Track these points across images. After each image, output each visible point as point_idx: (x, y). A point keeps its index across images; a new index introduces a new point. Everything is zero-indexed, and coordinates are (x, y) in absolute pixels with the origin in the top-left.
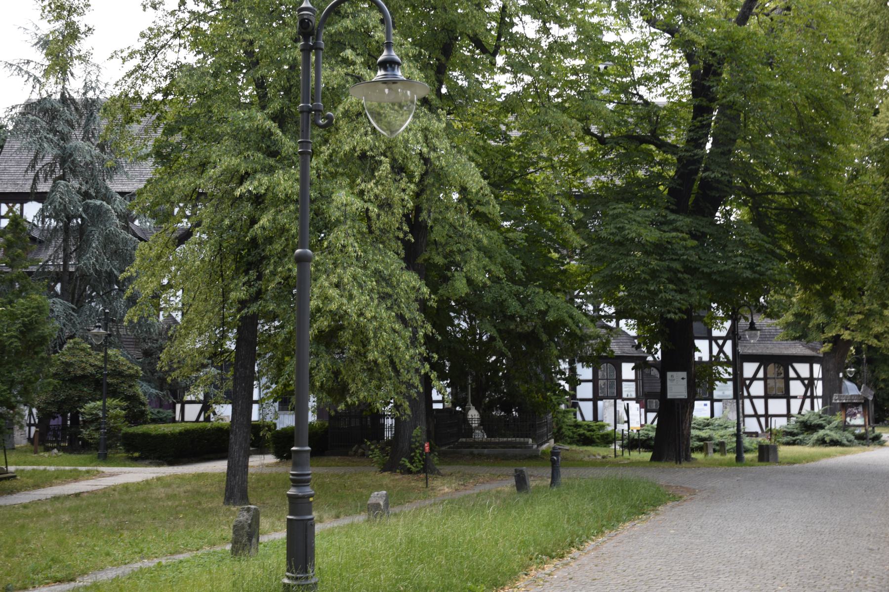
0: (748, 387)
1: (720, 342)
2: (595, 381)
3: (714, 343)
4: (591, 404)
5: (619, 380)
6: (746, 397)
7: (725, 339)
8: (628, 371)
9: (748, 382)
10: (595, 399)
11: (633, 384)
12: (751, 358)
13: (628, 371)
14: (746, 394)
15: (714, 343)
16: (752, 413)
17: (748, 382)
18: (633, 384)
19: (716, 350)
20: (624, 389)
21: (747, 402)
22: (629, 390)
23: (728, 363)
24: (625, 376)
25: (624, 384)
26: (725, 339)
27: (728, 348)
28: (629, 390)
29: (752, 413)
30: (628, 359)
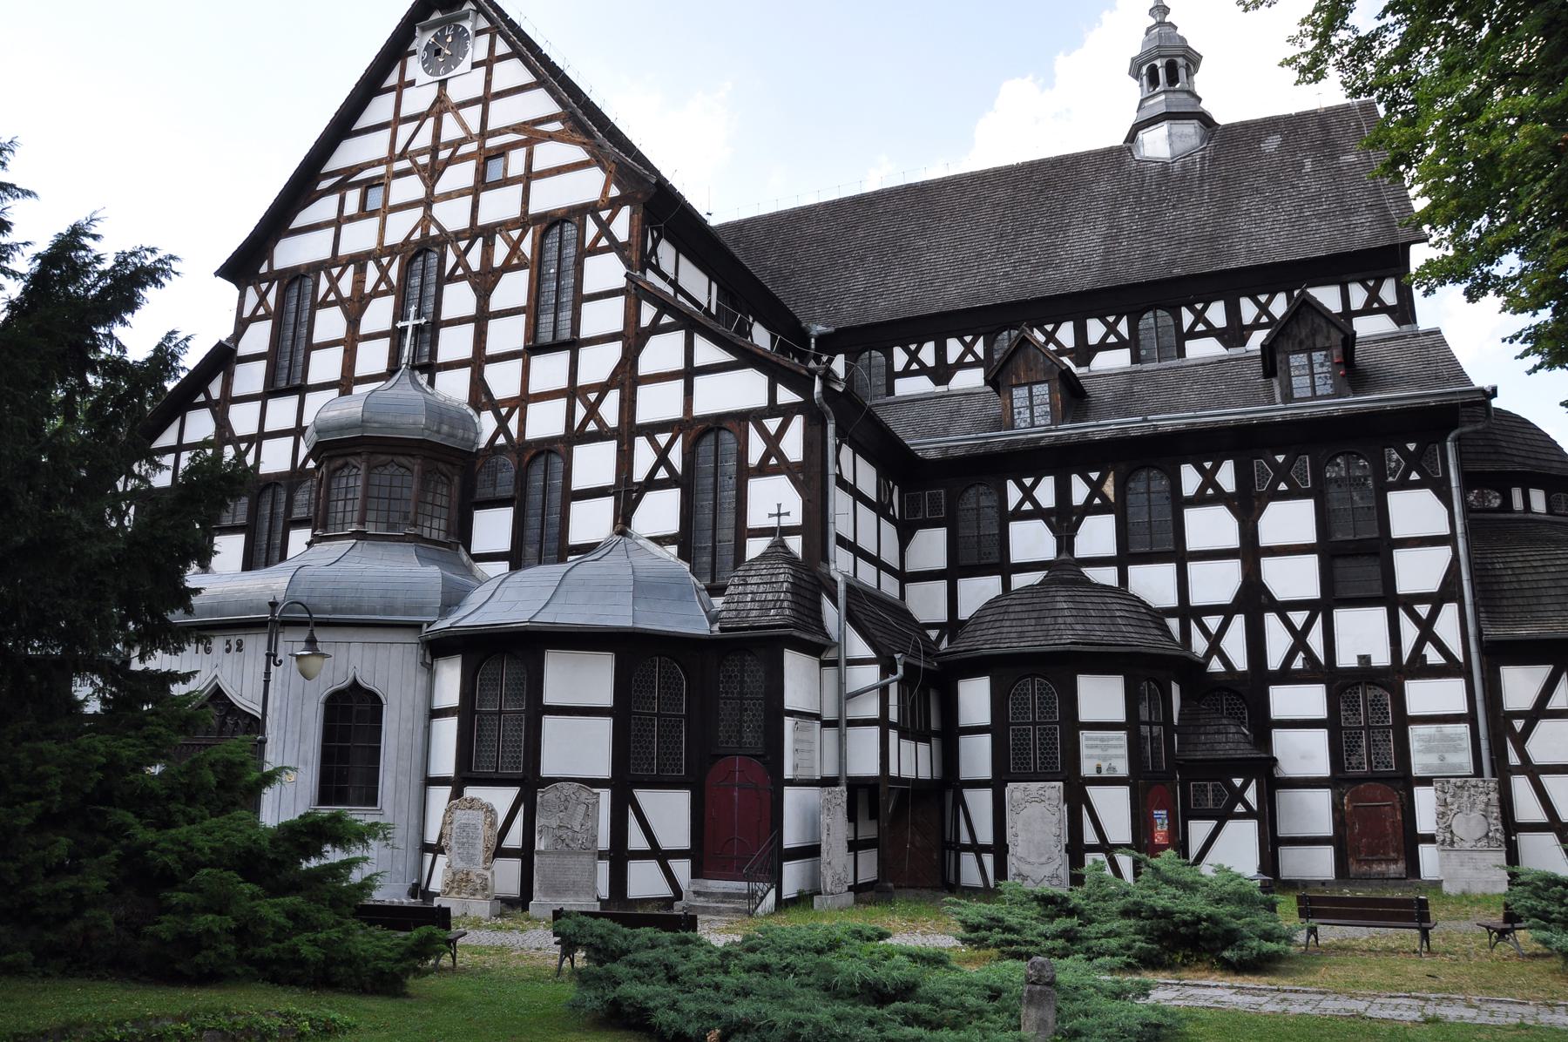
0: (1521, 740)
1: (1423, 610)
2: (998, 728)
3: (1402, 614)
4: (986, 795)
5: (1072, 725)
6: (1518, 770)
7: (1436, 600)
8: (1101, 697)
9: (1519, 724)
10: (997, 785)
11: (1122, 734)
12: (1524, 653)
13: (1101, 697)
14: (1514, 759)
15: (1402, 614)
16: (1540, 816)
17: (1519, 724)
18: (1122, 734)
19: (1409, 633)
20: (1084, 751)
21: (1521, 786)
22: (1104, 753)
23: (1451, 669)
24: (1088, 710)
25: (1084, 736)
26: (1436, 600)
27: (1448, 624)
28: (1104, 753)
29: (1540, 816)
30: (1100, 663)
